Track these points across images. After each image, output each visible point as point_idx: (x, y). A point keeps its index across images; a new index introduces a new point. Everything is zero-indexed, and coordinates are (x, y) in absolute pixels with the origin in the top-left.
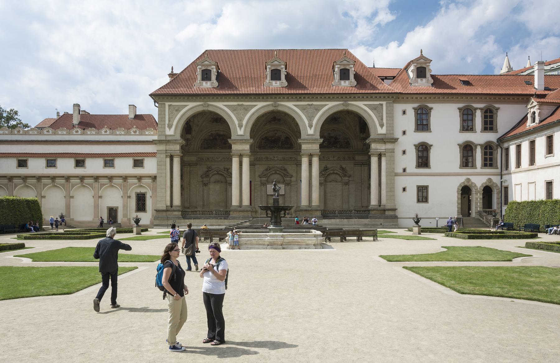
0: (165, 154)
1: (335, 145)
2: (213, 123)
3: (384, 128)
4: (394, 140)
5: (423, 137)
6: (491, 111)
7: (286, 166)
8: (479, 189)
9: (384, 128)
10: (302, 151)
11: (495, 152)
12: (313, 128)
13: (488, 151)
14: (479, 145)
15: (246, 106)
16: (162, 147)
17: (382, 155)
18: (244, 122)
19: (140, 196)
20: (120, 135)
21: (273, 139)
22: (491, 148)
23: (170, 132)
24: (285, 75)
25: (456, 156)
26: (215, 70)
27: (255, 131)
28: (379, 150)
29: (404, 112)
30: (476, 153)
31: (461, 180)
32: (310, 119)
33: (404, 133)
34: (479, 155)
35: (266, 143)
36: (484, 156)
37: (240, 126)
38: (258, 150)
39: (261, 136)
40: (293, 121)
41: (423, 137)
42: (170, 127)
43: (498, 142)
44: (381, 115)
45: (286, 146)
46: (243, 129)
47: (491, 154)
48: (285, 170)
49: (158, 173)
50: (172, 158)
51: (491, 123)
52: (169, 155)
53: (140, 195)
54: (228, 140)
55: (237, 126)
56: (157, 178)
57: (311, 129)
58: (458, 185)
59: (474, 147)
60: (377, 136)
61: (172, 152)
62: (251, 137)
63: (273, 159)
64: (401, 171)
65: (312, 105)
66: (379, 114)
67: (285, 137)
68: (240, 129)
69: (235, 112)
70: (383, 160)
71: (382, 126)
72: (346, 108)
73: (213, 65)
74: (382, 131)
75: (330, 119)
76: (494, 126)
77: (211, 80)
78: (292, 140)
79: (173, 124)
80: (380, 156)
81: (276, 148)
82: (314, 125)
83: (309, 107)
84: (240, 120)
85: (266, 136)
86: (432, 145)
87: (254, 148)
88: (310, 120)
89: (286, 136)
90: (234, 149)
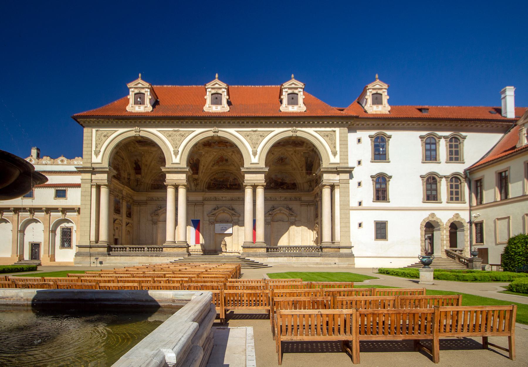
0: (90, 184)
3: (338, 156)
4: (349, 171)
5: (380, 167)
7: (234, 207)
8: (446, 225)
9: (338, 156)
10: (245, 181)
12: (257, 156)
13: (454, 183)
14: (445, 176)
15: (182, 132)
16: (88, 176)
17: (336, 187)
18: (181, 149)
19: (65, 231)
20: (46, 164)
23: (97, 160)
24: (226, 100)
28: (332, 181)
29: (359, 141)
30: (440, 185)
32: (255, 145)
33: (359, 163)
34: (443, 188)
36: (449, 190)
37: (176, 153)
38: (206, 190)
39: (210, 177)
41: (380, 167)
42: (97, 153)
43: (464, 172)
44: (333, 142)
46: (179, 156)
47: (457, 186)
48: (233, 209)
49: (81, 204)
50: (98, 187)
52: (94, 185)
53: (65, 230)
54: (161, 168)
55: (172, 153)
56: (81, 210)
57: (255, 157)
58: (422, 220)
59: (438, 179)
60: (330, 165)
61: (98, 181)
63: (221, 199)
64: (357, 205)
65: (256, 131)
66: (332, 141)
68: (176, 157)
69: (170, 138)
70: (337, 191)
71: (335, 154)
72: (294, 134)
73: (146, 88)
74: (335, 160)
77: (144, 104)
79: (100, 151)
80: (332, 187)
82: (258, 153)
83: (253, 133)
84: (176, 147)
86: (390, 177)
88: (255, 148)
90: (168, 179)
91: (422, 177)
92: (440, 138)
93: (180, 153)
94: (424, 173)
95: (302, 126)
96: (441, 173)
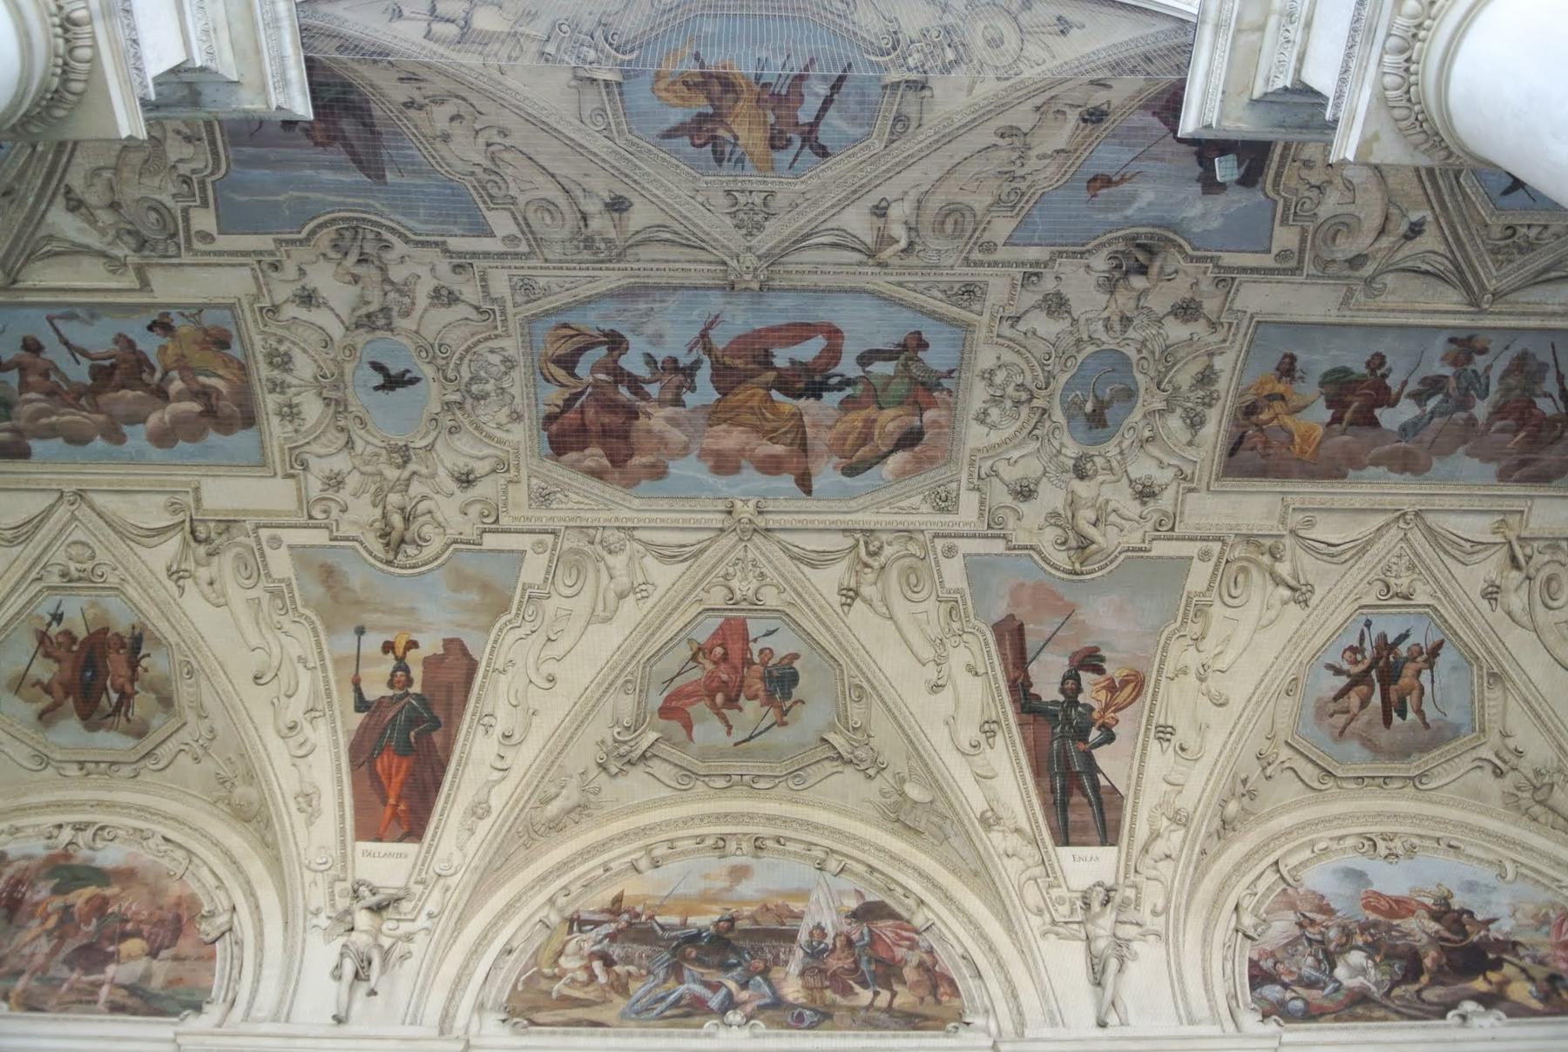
1: (1479, 985)
2: (46, 717)
21: (704, 920)
27: (496, 802)
35: (608, 962)
40: (936, 688)
45: (864, 996)
67: (852, 904)
75: (1338, 672)
78: (942, 938)
81: (734, 1017)
85: (618, 899)
87: (446, 1018)
89: (860, 894)
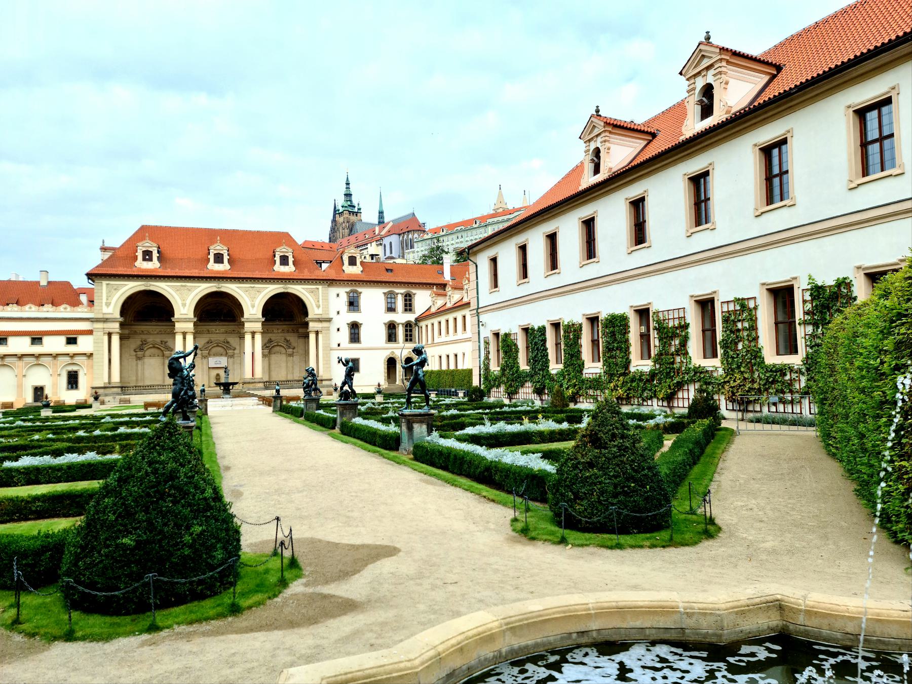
6: (410, 296)
11: (414, 330)
13: (408, 328)
18: (188, 302)
22: (411, 326)
25: (383, 333)
26: (156, 251)
31: (386, 354)
34: (400, 332)
37: (184, 305)
47: (411, 331)
51: (410, 305)
55: (181, 305)
62: (195, 316)
76: (413, 308)
91: (385, 324)
92: (397, 294)
93: (187, 305)
94: (386, 322)
95: (291, 284)
96: (398, 321)
